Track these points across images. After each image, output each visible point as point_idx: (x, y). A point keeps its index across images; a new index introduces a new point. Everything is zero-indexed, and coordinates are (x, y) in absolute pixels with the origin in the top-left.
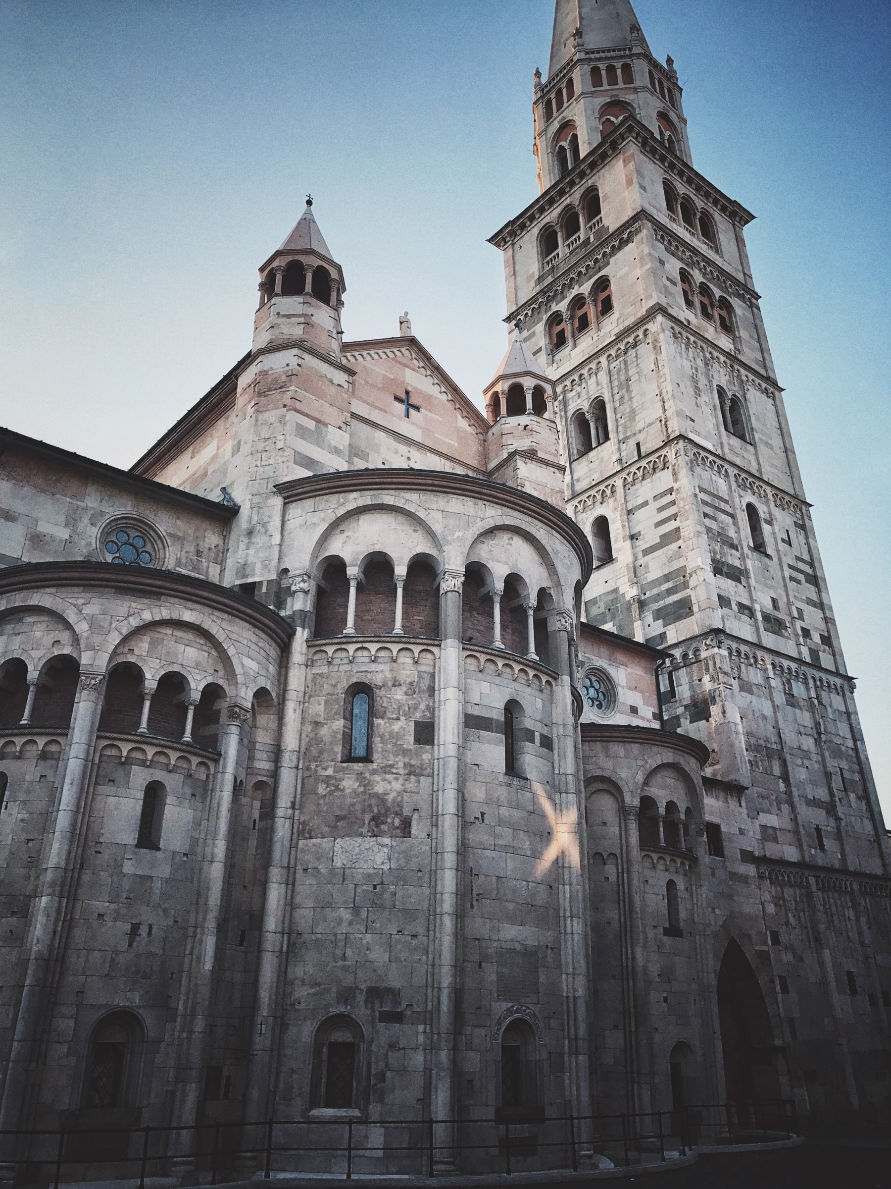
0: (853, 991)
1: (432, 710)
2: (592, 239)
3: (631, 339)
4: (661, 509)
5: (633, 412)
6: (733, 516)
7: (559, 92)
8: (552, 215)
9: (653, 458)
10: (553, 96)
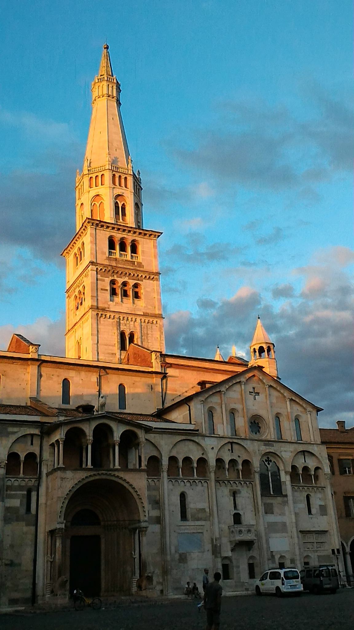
2: (136, 263)
3: (151, 320)
8: (118, 236)
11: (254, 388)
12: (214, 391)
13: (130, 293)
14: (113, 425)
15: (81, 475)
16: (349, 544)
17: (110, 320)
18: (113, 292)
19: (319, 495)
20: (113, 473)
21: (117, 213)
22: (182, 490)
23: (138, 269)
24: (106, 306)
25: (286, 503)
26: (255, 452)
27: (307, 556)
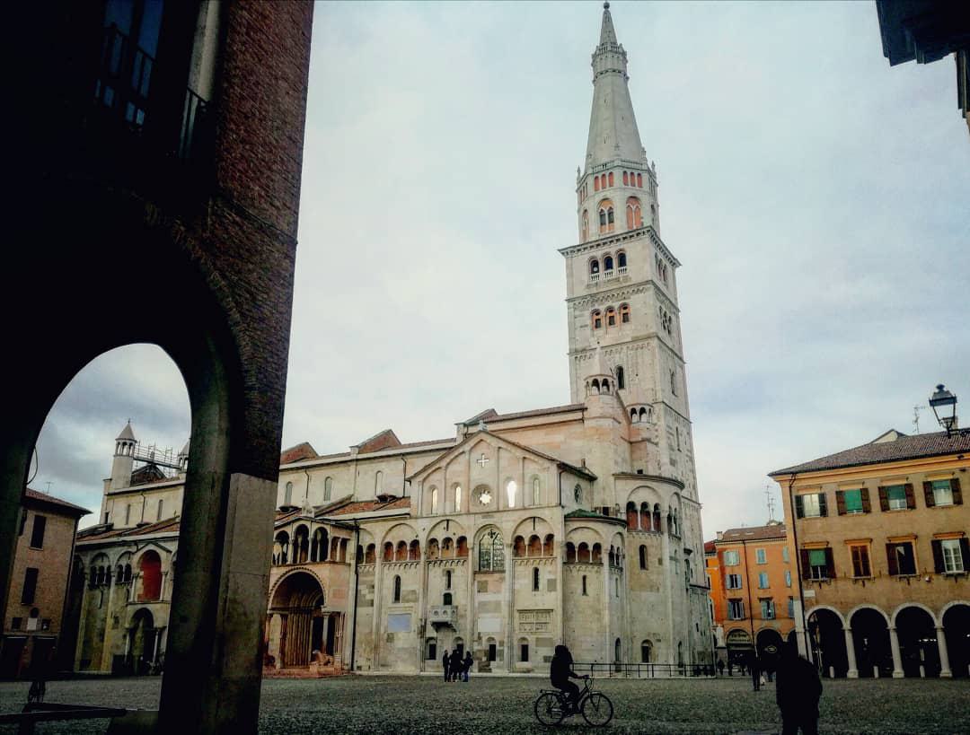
1: (661, 554)
3: (640, 344)
6: (673, 435)
8: (599, 254)
10: (600, 175)
12: (434, 468)
13: (618, 318)
14: (308, 524)
15: (283, 570)
16: (895, 615)
18: (597, 324)
19: (549, 568)
20: (304, 567)
21: (602, 224)
22: (397, 574)
23: (624, 284)
24: (587, 344)
25: (503, 579)
26: (467, 527)
27: (524, 639)
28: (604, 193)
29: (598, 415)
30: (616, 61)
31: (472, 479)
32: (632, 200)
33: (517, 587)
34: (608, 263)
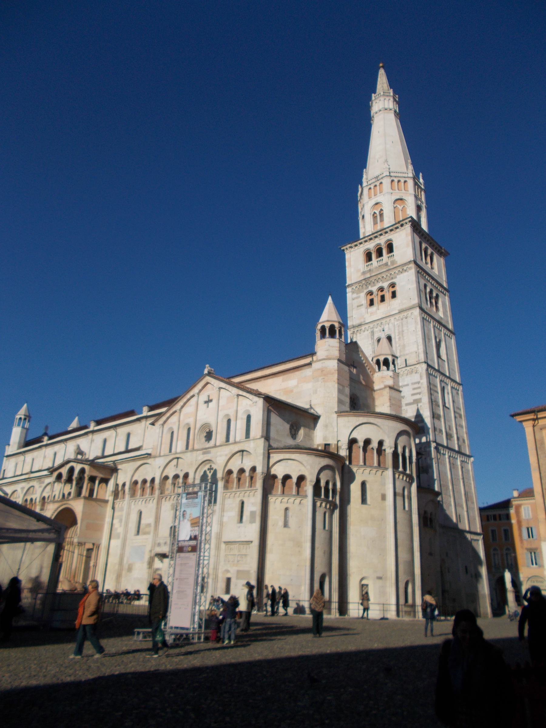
0: (467, 572)
2: (389, 264)
4: (414, 389)
5: (404, 346)
7: (376, 186)
8: (371, 245)
9: (412, 367)
10: (372, 186)
11: (209, 396)
13: (388, 296)
17: (366, 332)
18: (372, 303)
21: (375, 223)
23: (392, 267)
24: (362, 320)
28: (376, 199)
29: (324, 357)
30: (386, 102)
31: (198, 418)
32: (399, 201)
33: (225, 519)
34: (379, 253)
